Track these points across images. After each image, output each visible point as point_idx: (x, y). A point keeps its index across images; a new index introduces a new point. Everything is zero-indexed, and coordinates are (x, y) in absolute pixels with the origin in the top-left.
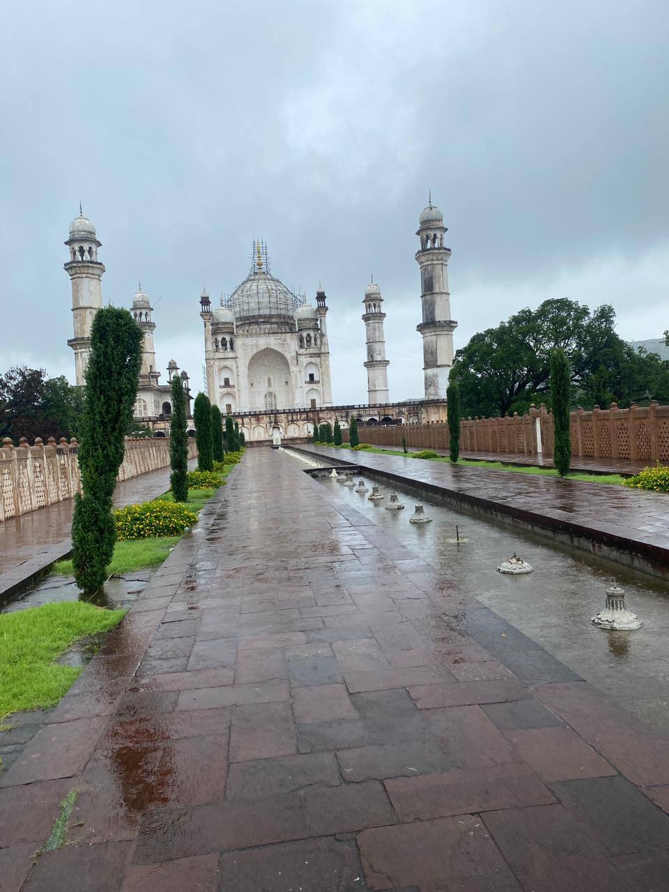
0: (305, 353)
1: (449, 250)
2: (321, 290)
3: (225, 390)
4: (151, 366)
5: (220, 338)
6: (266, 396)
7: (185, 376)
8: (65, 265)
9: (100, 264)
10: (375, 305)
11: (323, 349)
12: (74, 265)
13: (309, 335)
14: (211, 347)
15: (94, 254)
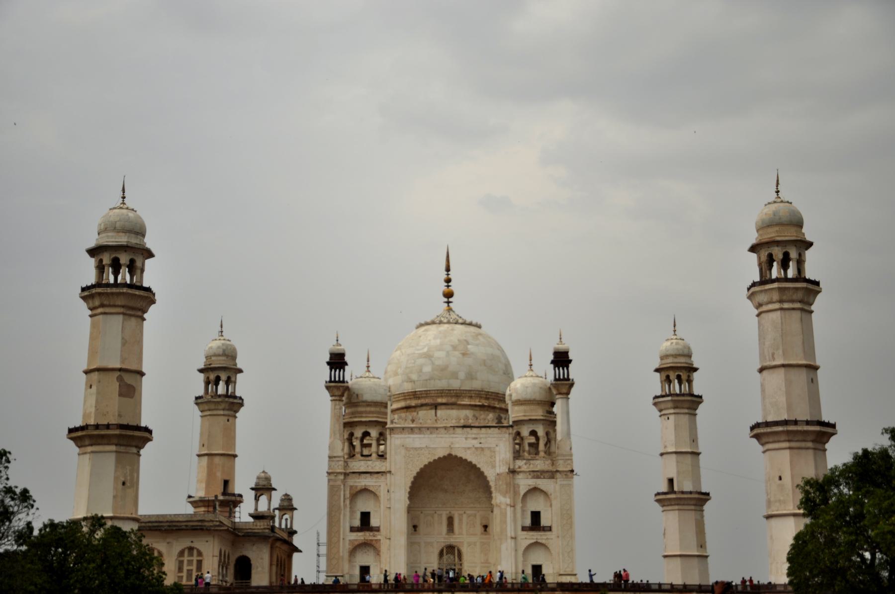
0: (525, 468)
1: (817, 283)
2: (561, 347)
3: (360, 536)
4: (226, 483)
5: (358, 433)
6: (441, 554)
7: (287, 506)
8: (83, 289)
9: (148, 290)
10: (679, 378)
11: (561, 462)
12: (99, 290)
13: (533, 433)
14: (341, 449)
15: (139, 272)
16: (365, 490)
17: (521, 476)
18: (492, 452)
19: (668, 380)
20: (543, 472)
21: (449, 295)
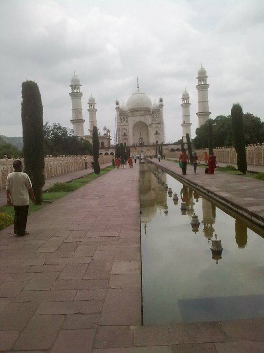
3: (124, 137)
7: (109, 131)
14: (119, 121)
16: (124, 128)
17: (154, 124)
18: (148, 120)
19: (184, 100)
20: (157, 123)
21: (138, 87)
